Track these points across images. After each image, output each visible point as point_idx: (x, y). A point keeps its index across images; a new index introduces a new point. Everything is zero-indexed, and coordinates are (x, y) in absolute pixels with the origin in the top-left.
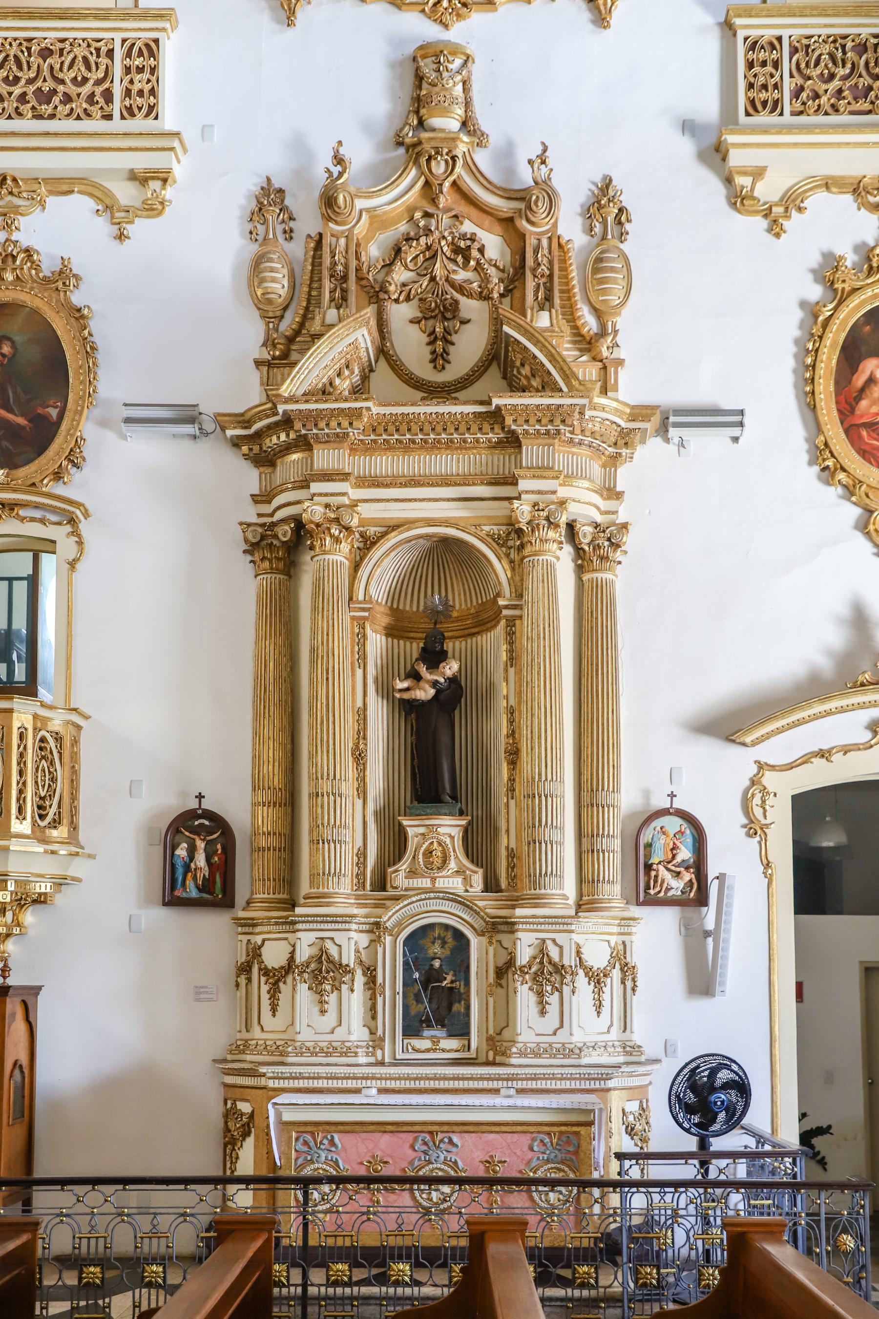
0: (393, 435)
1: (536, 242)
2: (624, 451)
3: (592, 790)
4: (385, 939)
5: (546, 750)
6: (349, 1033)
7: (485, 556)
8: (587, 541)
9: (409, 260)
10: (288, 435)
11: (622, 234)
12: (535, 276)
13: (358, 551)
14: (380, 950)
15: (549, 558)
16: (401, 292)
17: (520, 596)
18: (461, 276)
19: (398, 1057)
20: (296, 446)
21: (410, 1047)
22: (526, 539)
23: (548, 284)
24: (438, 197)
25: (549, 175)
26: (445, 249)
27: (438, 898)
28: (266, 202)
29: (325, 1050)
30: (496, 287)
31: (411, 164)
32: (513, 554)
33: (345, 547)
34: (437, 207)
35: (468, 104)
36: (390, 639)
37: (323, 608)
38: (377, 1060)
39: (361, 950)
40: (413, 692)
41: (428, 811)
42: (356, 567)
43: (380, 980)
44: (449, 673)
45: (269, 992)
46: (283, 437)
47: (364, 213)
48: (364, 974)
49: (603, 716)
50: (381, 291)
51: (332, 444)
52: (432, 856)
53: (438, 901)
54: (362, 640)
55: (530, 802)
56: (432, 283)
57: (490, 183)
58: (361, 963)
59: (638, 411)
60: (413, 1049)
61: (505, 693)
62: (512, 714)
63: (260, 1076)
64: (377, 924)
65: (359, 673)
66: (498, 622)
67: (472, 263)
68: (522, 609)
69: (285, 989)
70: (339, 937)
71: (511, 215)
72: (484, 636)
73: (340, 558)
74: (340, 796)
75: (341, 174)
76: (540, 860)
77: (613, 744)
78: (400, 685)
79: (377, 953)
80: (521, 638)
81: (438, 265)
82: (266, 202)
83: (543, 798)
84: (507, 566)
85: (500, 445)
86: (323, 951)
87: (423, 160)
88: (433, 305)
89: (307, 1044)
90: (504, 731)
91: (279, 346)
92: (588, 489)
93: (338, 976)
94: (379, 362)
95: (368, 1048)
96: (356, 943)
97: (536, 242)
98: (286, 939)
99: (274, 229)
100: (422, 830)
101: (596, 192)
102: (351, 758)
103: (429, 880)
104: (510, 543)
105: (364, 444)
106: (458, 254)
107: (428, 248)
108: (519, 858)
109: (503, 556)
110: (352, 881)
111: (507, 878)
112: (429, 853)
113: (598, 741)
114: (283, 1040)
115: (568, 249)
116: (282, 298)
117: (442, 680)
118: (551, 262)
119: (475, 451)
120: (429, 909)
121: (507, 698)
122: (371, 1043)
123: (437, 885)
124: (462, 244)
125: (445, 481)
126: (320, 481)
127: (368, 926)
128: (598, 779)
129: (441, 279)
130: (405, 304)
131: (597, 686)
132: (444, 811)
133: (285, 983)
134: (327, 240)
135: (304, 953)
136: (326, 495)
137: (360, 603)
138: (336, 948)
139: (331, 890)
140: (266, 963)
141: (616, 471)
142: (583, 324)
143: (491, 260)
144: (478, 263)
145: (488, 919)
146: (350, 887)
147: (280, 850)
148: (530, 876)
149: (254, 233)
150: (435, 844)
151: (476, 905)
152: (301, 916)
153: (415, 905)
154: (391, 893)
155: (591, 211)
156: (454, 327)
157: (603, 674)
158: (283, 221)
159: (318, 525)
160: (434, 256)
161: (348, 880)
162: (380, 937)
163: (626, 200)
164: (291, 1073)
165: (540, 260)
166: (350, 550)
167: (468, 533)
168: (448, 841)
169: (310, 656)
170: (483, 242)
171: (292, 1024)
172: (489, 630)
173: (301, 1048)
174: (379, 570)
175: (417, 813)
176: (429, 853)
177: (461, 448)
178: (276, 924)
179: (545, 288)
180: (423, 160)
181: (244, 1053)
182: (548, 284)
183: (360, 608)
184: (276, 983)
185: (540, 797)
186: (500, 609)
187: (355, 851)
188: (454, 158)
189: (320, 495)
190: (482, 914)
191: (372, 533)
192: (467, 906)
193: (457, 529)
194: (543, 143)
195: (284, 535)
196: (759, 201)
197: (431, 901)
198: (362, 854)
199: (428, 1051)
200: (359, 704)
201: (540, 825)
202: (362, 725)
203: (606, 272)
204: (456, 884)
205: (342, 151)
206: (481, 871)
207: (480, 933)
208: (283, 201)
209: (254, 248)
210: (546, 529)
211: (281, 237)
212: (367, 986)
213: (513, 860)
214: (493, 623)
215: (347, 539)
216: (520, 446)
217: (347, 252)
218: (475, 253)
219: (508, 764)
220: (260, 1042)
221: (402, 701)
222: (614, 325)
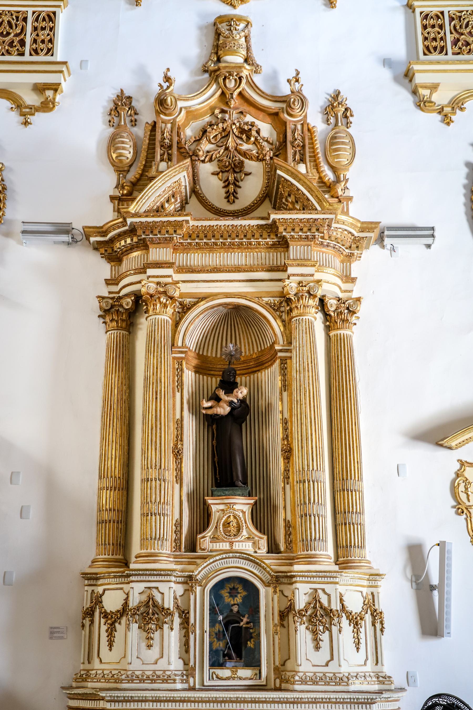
1: (293, 126)
2: (356, 252)
3: (343, 479)
4: (196, 588)
5: (312, 448)
6: (169, 663)
7: (265, 317)
8: (333, 309)
9: (211, 137)
11: (348, 123)
12: (293, 146)
13: (178, 314)
14: (192, 597)
16: (206, 156)
17: (290, 343)
18: (245, 147)
20: (137, 247)
23: (302, 151)
24: (230, 101)
26: (235, 130)
27: (236, 557)
28: (120, 104)
29: (151, 677)
30: (268, 153)
32: (285, 316)
33: (170, 310)
34: (230, 107)
35: (248, 49)
37: (154, 351)
38: (189, 686)
39: (178, 597)
40: (215, 409)
41: (227, 493)
42: (177, 324)
43: (192, 621)
44: (240, 396)
48: (180, 617)
49: (348, 427)
50: (193, 155)
52: (229, 526)
53: (235, 559)
54: (180, 373)
55: (301, 486)
56: (226, 151)
58: (178, 607)
60: (217, 677)
61: (280, 409)
62: (286, 423)
63: (99, 700)
64: (190, 577)
65: (178, 395)
66: (275, 361)
67: (253, 139)
68: (291, 352)
69: (120, 628)
70: (163, 587)
71: (277, 111)
73: (166, 318)
74: (164, 481)
77: (357, 447)
79: (190, 599)
80: (291, 372)
81: (230, 140)
82: (120, 104)
83: (311, 483)
84: (280, 324)
86: (151, 598)
88: (227, 163)
89: (137, 673)
90: (281, 436)
91: (126, 187)
92: (333, 274)
93: (161, 617)
94: (192, 198)
95: (183, 676)
96: (174, 592)
97: (293, 126)
99: (125, 120)
100: (222, 507)
101: (330, 99)
102: (171, 454)
103: (228, 544)
104: (282, 309)
106: (243, 134)
107: (224, 130)
108: (295, 528)
109: (277, 317)
110: (171, 545)
111: (286, 543)
112: (227, 524)
113: (346, 444)
114: (117, 670)
115: (314, 131)
116: (129, 160)
117: (236, 401)
118: (303, 138)
120: (228, 565)
121: (282, 412)
122: (185, 672)
123: (234, 548)
124: (246, 128)
125: (238, 269)
127: (183, 579)
128: (347, 471)
129: (232, 148)
131: (344, 406)
132: (239, 493)
133: (120, 623)
135: (134, 602)
137: (180, 348)
138: (160, 595)
139: (157, 551)
142: (325, 176)
143: (264, 138)
144: (256, 139)
145: (272, 574)
146: (170, 549)
149: (112, 122)
150: (232, 517)
151: (264, 563)
153: (218, 562)
154: (200, 553)
155: (328, 109)
157: (347, 398)
158: (131, 115)
160: (228, 135)
161: (169, 543)
162: (192, 587)
163: (349, 104)
165: (296, 137)
166: (173, 313)
167: (253, 302)
168: (241, 515)
169: (144, 383)
170: (259, 127)
171: (125, 657)
173: (132, 676)
174: (192, 326)
175: (219, 494)
176: (227, 524)
179: (300, 153)
182: (302, 151)
183: (179, 351)
185: (309, 482)
186: (276, 352)
187: (174, 522)
190: (268, 569)
191: (188, 302)
192: (257, 563)
193: (246, 299)
196: (435, 103)
197: (230, 559)
198: (179, 524)
200: (178, 416)
202: (180, 432)
203: (339, 145)
204: (248, 547)
206: (265, 537)
208: (131, 103)
209: (112, 130)
211: (129, 125)
212: (182, 626)
213: (289, 529)
215: (171, 305)
217: (172, 132)
218: (254, 133)
219: (284, 459)
222: (345, 177)
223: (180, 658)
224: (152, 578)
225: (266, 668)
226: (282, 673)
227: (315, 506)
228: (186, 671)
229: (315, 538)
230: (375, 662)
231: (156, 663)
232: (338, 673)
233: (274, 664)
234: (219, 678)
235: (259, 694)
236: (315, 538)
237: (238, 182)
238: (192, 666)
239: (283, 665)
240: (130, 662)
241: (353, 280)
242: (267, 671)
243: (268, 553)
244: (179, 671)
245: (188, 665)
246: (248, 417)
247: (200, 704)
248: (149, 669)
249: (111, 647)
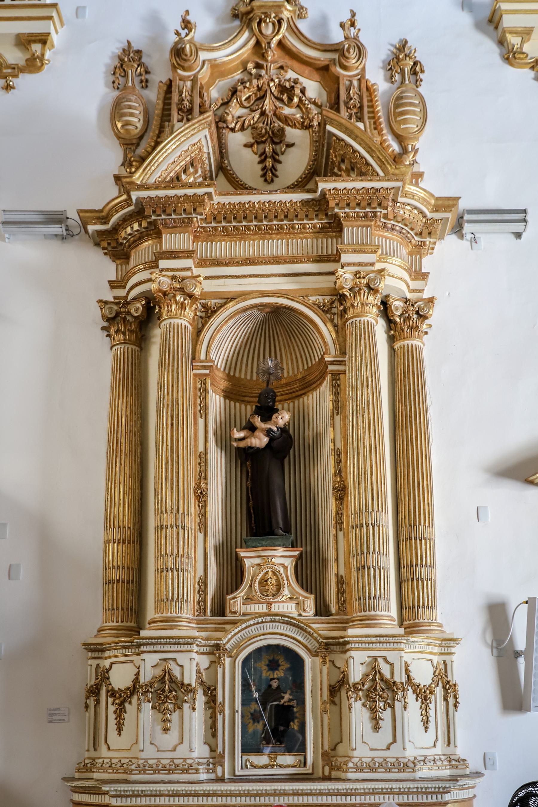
0: (231, 222)
1: (347, 83)
2: (428, 240)
4: (224, 660)
5: (372, 484)
6: (191, 750)
7: (312, 321)
8: (399, 313)
9: (243, 98)
10: (140, 225)
11: (417, 81)
12: (348, 108)
13: (200, 320)
14: (220, 671)
15: (370, 319)
16: (237, 123)
17: (344, 353)
18: (287, 111)
19: (237, 773)
20: (147, 235)
21: (248, 764)
22: (349, 304)
23: (359, 114)
24: (267, 52)
25: (357, 34)
26: (273, 89)
27: (274, 621)
28: (126, 59)
29: (168, 766)
30: (316, 116)
31: (245, 27)
32: (337, 320)
33: (189, 313)
34: (267, 61)
36: (227, 401)
37: (169, 364)
38: (217, 776)
39: (202, 671)
40: (249, 440)
41: (264, 543)
42: (199, 332)
43: (220, 699)
44: (281, 423)
45: (115, 712)
46: (136, 226)
47: (206, 62)
48: (205, 694)
50: (220, 121)
51: (178, 229)
52: (267, 584)
53: (274, 624)
54: (203, 394)
55: (358, 532)
56: (262, 117)
57: (309, 41)
58: (202, 683)
59: (440, 202)
60: (252, 765)
61: (332, 437)
62: (339, 455)
64: (217, 647)
65: (201, 422)
66: (324, 378)
67: (296, 100)
68: (345, 365)
69: (131, 708)
70: (182, 658)
71: (327, 63)
72: (311, 396)
73: (184, 323)
74: (183, 528)
75: (187, 35)
76: (369, 584)
78: (238, 434)
79: (217, 674)
80: (345, 390)
81: (267, 101)
82: (126, 59)
83: (371, 527)
84: (331, 328)
85: (323, 230)
86: (167, 672)
87: (255, 26)
88: (264, 131)
89: (150, 762)
90: (332, 471)
91: (134, 163)
92: (399, 266)
93: (181, 695)
94: (219, 175)
95: (208, 765)
96: (197, 664)
97: (347, 83)
98: (131, 662)
99: (132, 80)
100: (258, 561)
101: (395, 51)
102: (193, 496)
103: (265, 605)
104: (334, 310)
105: (206, 231)
106: (283, 95)
107: (259, 89)
108: (349, 585)
109: (328, 320)
110: (194, 608)
111: (338, 603)
112: (264, 582)
114: (128, 758)
115: (374, 90)
116: (138, 130)
117: (275, 429)
118: (361, 97)
119: (301, 236)
120: (266, 631)
121: (334, 441)
122: (211, 760)
123: (272, 610)
124: (287, 85)
125: (277, 260)
126: (168, 258)
127: (208, 648)
129: (270, 112)
130: (240, 133)
132: (278, 543)
133: (130, 703)
134: (177, 82)
135: (146, 676)
136: (172, 270)
137: (203, 361)
138: (178, 668)
139: (174, 615)
140: (113, 685)
141: (421, 258)
142: (388, 146)
143: (311, 99)
144: (300, 100)
145: (321, 640)
146: (192, 612)
147: (128, 583)
148: (360, 599)
149: (116, 82)
150: (270, 573)
151: (310, 627)
152: (146, 638)
153: (252, 628)
154: (229, 617)
155: (391, 63)
156: (281, 149)
158: (140, 75)
159: (165, 294)
160: (263, 97)
161: (190, 606)
162: (219, 658)
163: (419, 56)
164: (133, 791)
165: (352, 95)
166: (194, 318)
167: (297, 301)
168: (282, 570)
170: (304, 85)
171: (137, 743)
172: (315, 389)
173: (144, 766)
174: (218, 336)
176: (264, 582)
177: (290, 233)
178: (123, 647)
179: (357, 117)
180: (255, 26)
181: (91, 771)
182: (359, 114)
184: (122, 704)
185: (367, 526)
186: (326, 365)
187: (197, 580)
188: (280, 22)
189: (167, 270)
190: (315, 635)
191: (212, 304)
192: (301, 628)
193: (288, 298)
194: (352, 11)
195: (137, 310)
196: (527, 56)
197: (268, 624)
198: (203, 583)
199: (266, 766)
200: (201, 448)
201: (368, 551)
202: (203, 468)
203: (407, 106)
204: (290, 609)
205: (188, 18)
206: (312, 597)
207: (314, 654)
208: (140, 59)
209: (116, 93)
210: (366, 294)
211: (138, 87)
212: (207, 705)
213: (342, 587)
214: (318, 382)
215: (191, 307)
216: (341, 231)
217: (192, 91)
218: (297, 91)
219: (336, 499)
220: (106, 761)
221: (238, 449)
222: (413, 147)
223: (205, 743)
224: (169, 648)
225: (312, 753)
226: (332, 759)
227: (375, 557)
228: (212, 758)
229: (375, 596)
230: (446, 743)
231: (175, 750)
232: (402, 758)
233: (322, 748)
235: (303, 786)
236: (375, 596)
237: (278, 155)
238: (220, 752)
239: (334, 749)
240: (142, 749)
241: (424, 276)
242: (313, 757)
243: (316, 615)
244: (205, 758)
246: (291, 451)
247: (229, 798)
248: (165, 758)
249: (119, 732)
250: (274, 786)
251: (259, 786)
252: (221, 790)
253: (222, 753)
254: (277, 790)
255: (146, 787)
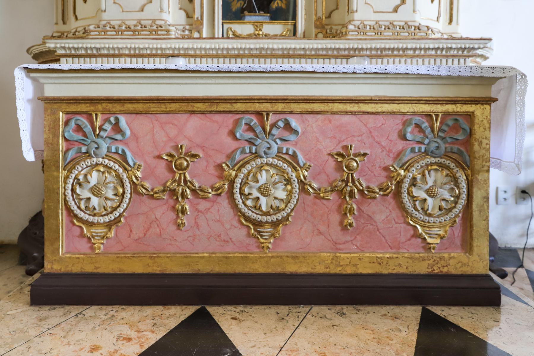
29: (132, 28)
60: (234, 34)
89: (113, 23)
95: (184, 31)
122: (187, 27)
164: (86, 49)
199: (249, 37)
223: (180, 9)
225: (303, 20)
226: (326, 27)
231: (142, 11)
232: (411, 21)
233: (316, 14)
234: (237, 36)
235: (295, 44)
238: (197, 18)
239: (329, 16)
240: (103, 9)
242: (305, 24)
244: (180, 25)
245: (192, 17)
248: (132, 18)
250: (260, 44)
251: (241, 43)
252: (193, 49)
253: (199, 19)
254: (263, 48)
255: (100, 43)
